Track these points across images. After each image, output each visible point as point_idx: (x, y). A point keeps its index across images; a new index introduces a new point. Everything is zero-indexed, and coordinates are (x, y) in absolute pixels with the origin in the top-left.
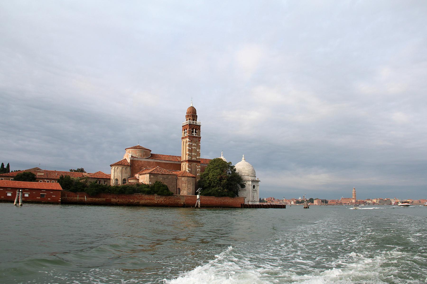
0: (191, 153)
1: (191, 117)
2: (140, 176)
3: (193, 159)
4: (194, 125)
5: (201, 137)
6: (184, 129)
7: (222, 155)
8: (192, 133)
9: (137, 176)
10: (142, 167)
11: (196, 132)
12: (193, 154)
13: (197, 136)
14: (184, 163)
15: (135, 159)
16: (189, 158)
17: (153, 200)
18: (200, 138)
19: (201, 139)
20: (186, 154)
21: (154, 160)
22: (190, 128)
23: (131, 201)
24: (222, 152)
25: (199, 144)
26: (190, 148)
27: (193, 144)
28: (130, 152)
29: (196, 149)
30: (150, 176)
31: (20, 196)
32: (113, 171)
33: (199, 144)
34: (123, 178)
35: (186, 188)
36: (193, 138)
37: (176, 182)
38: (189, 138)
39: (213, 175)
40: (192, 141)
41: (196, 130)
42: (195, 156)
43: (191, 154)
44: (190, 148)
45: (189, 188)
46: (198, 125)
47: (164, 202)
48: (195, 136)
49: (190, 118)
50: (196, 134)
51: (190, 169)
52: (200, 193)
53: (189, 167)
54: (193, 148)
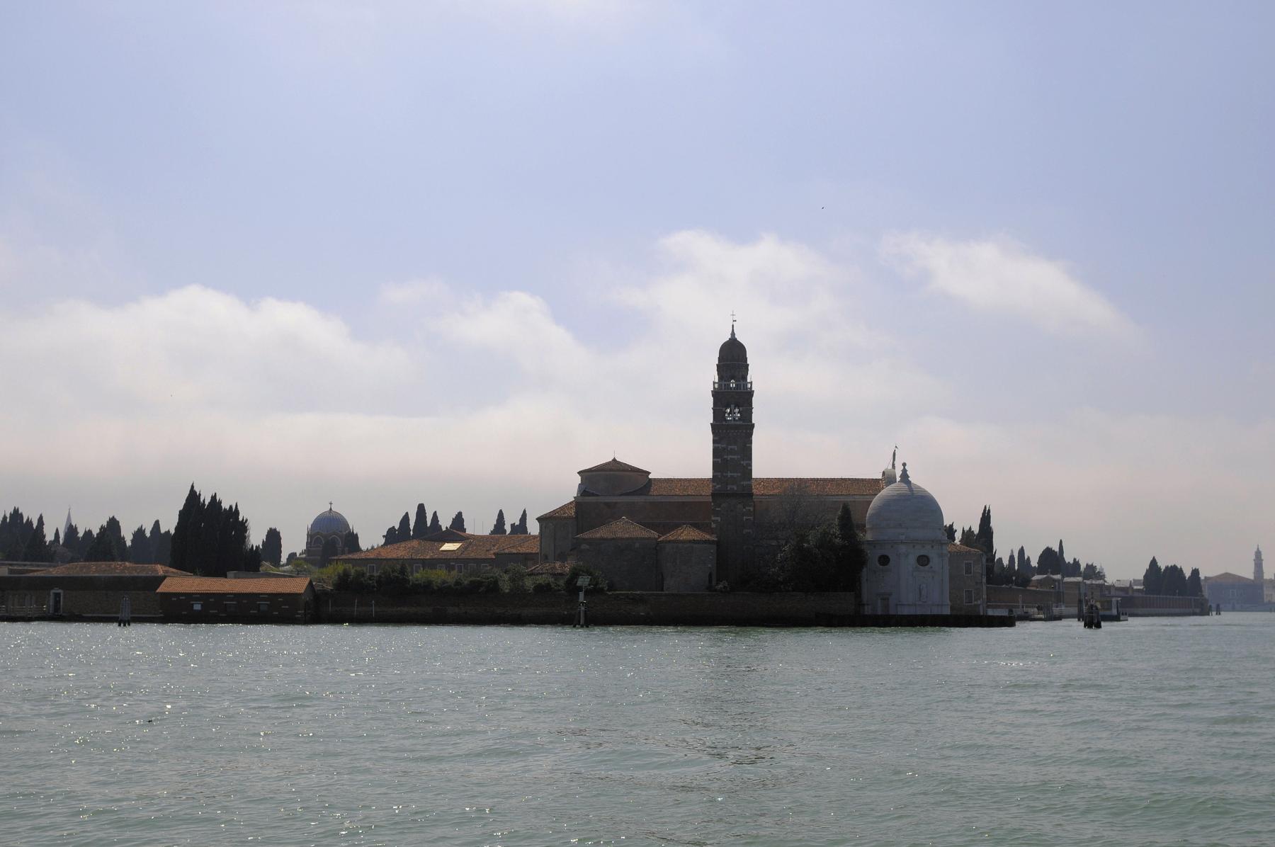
3: (729, 489)
12: (729, 474)
26: (719, 460)
27: (730, 447)
44: (719, 460)
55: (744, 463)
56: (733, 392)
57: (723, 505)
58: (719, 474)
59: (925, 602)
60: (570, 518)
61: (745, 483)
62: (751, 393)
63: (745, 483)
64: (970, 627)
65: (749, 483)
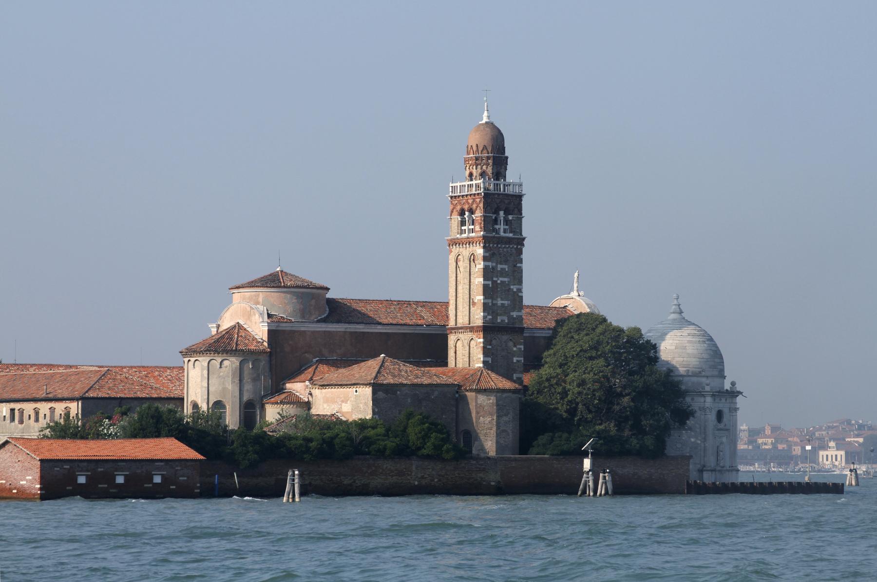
0: (492, 298)
1: (488, 165)
2: (317, 392)
3: (499, 321)
4: (499, 195)
5: (524, 239)
6: (459, 208)
7: (575, 285)
8: (493, 227)
9: (298, 388)
10: (306, 354)
11: (507, 222)
12: (500, 302)
13: (511, 235)
14: (461, 336)
15: (285, 327)
16: (487, 319)
17: (409, 477)
18: (520, 241)
19: (523, 245)
20: (471, 303)
21: (347, 326)
22: (489, 208)
23: (345, 482)
24: (576, 275)
25: (519, 265)
26: (490, 283)
27: (500, 267)
28: (260, 300)
29: (508, 285)
30: (374, 393)
31: (590, 481)
32: (202, 375)
33: (519, 265)
34: (245, 399)
35: (492, 431)
36: (498, 244)
37: (454, 409)
38: (484, 247)
39: (582, 383)
40: (493, 254)
41: (507, 213)
42: (506, 310)
43: (492, 302)
44: (490, 283)
45: (501, 429)
46: (512, 196)
47: (440, 480)
48: (503, 238)
49: (484, 167)
50: (507, 227)
51: (489, 359)
52: (592, 453)
53: (486, 352)
54: (499, 282)
55: (514, 288)
56: (502, 194)
57: (494, 342)
58: (490, 301)
59: (723, 467)
60: (263, 352)
61: (514, 314)
62: (519, 197)
63: (514, 314)
64: (831, 493)
65: (519, 314)
